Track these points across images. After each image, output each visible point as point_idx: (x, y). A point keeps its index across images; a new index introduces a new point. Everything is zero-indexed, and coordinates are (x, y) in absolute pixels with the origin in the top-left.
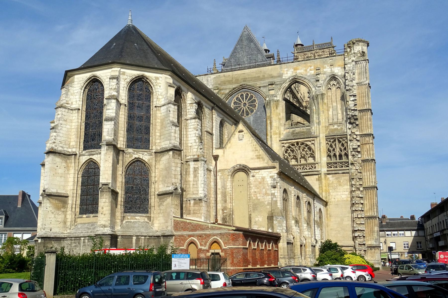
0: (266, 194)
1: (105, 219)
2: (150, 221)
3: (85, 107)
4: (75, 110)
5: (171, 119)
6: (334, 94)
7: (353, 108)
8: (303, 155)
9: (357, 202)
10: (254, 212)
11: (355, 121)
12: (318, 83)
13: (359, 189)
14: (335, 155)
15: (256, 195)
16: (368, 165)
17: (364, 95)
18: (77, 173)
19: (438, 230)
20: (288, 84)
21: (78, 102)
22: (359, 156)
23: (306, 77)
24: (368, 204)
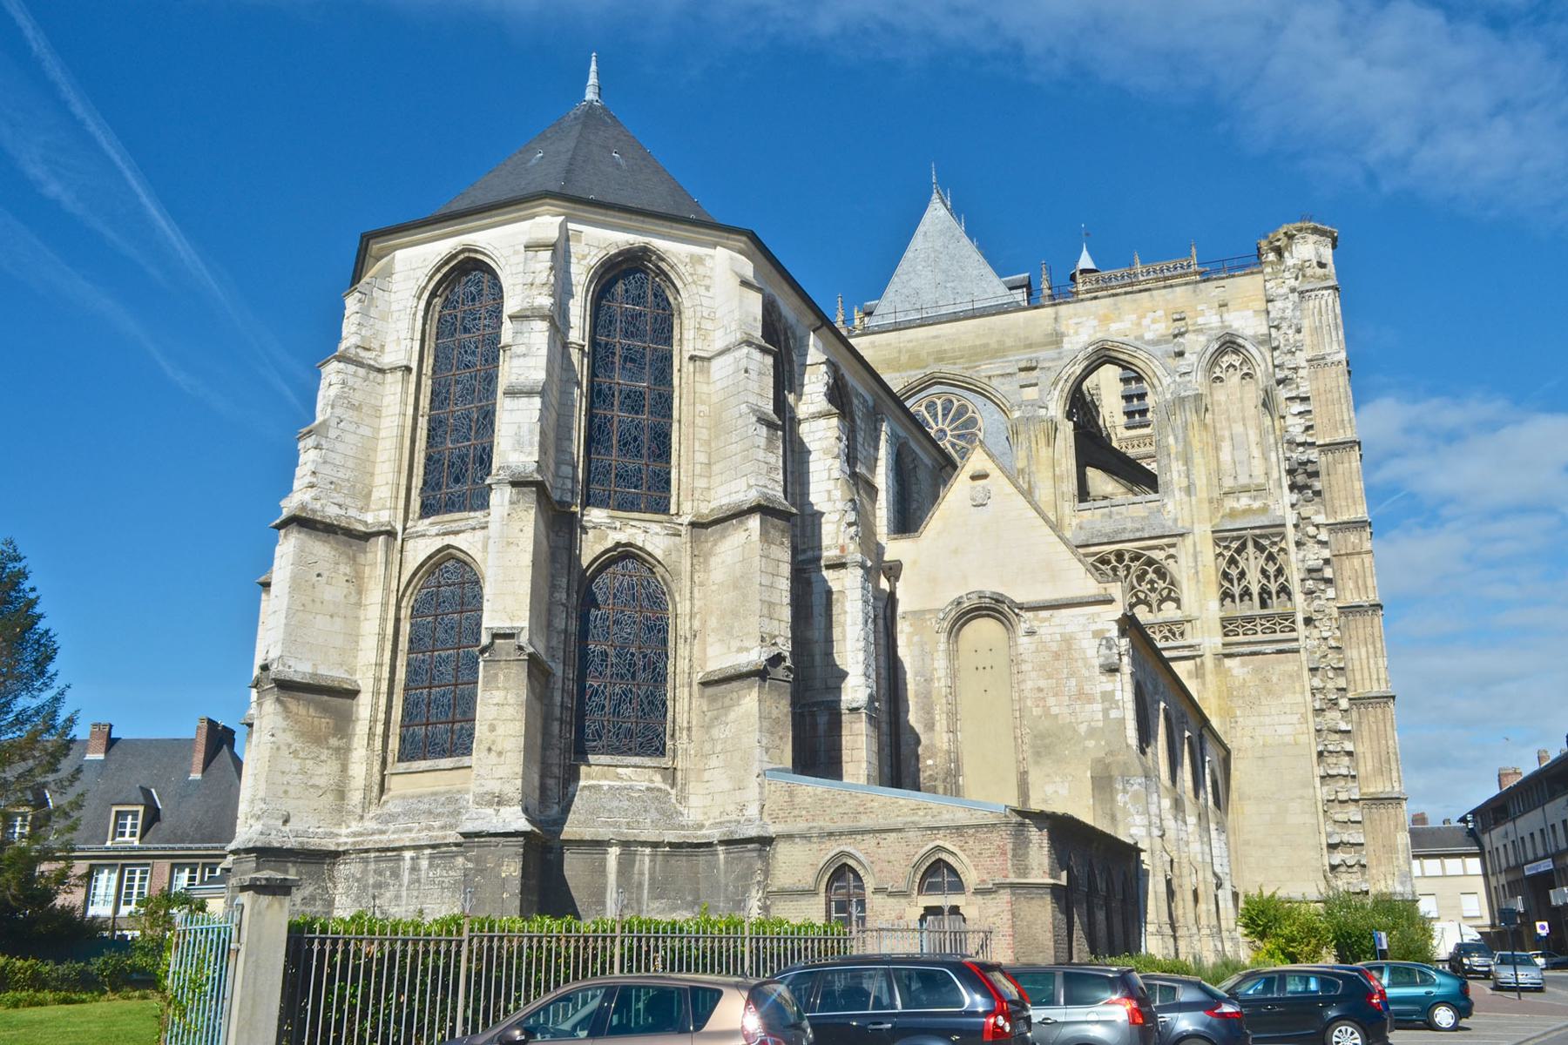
0: (1083, 696)
1: (502, 771)
2: (673, 785)
3: (431, 361)
4: (393, 370)
5: (753, 399)
6: (1235, 397)
7: (1300, 439)
8: (1142, 596)
9: (1331, 748)
10: (1037, 763)
11: (1309, 482)
12: (1180, 361)
13: (1334, 703)
14: (1246, 593)
15: (1044, 699)
16: (1361, 625)
17: (1336, 396)
18: (393, 601)
19: (1541, 853)
20: (1082, 366)
21: (404, 343)
22: (1331, 593)
23: (1138, 344)
24: (1368, 756)
